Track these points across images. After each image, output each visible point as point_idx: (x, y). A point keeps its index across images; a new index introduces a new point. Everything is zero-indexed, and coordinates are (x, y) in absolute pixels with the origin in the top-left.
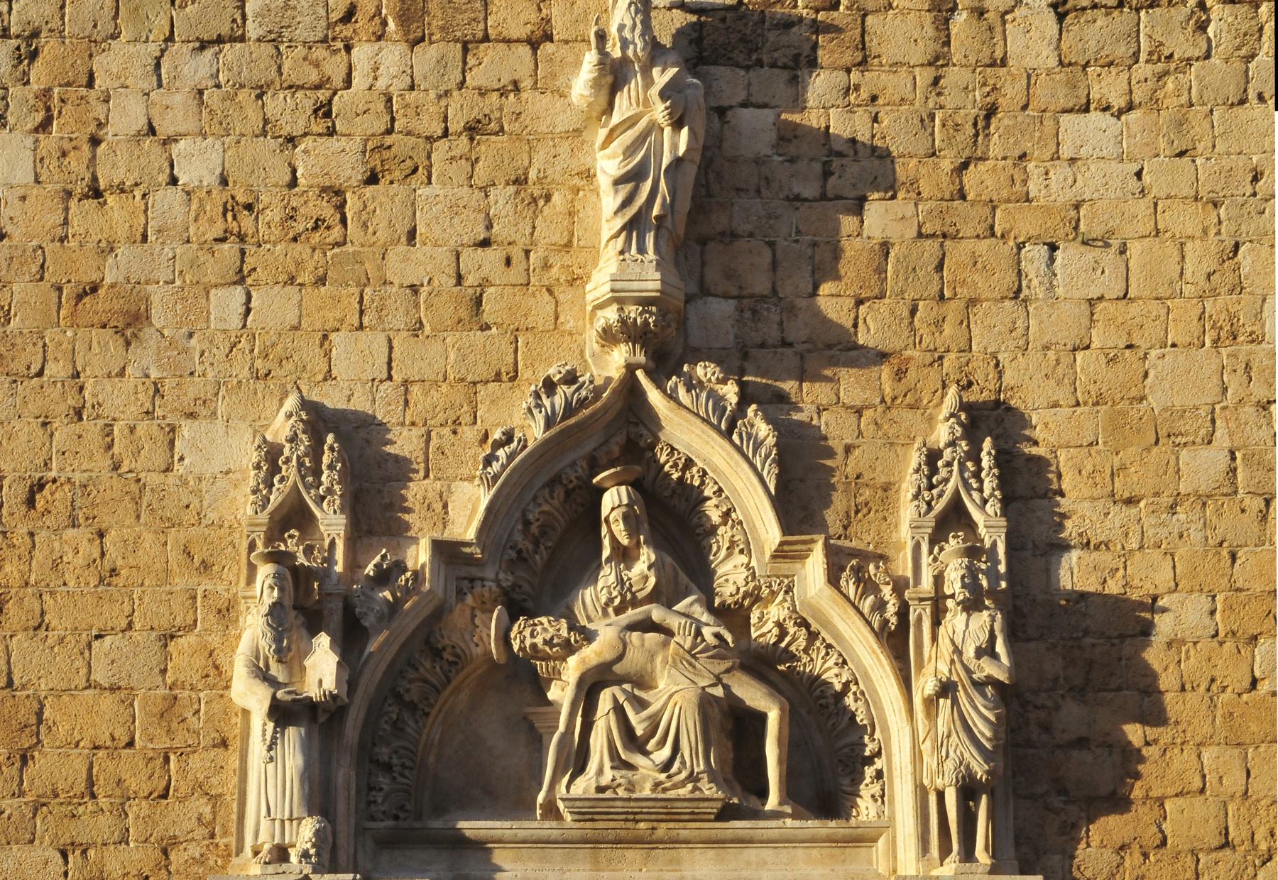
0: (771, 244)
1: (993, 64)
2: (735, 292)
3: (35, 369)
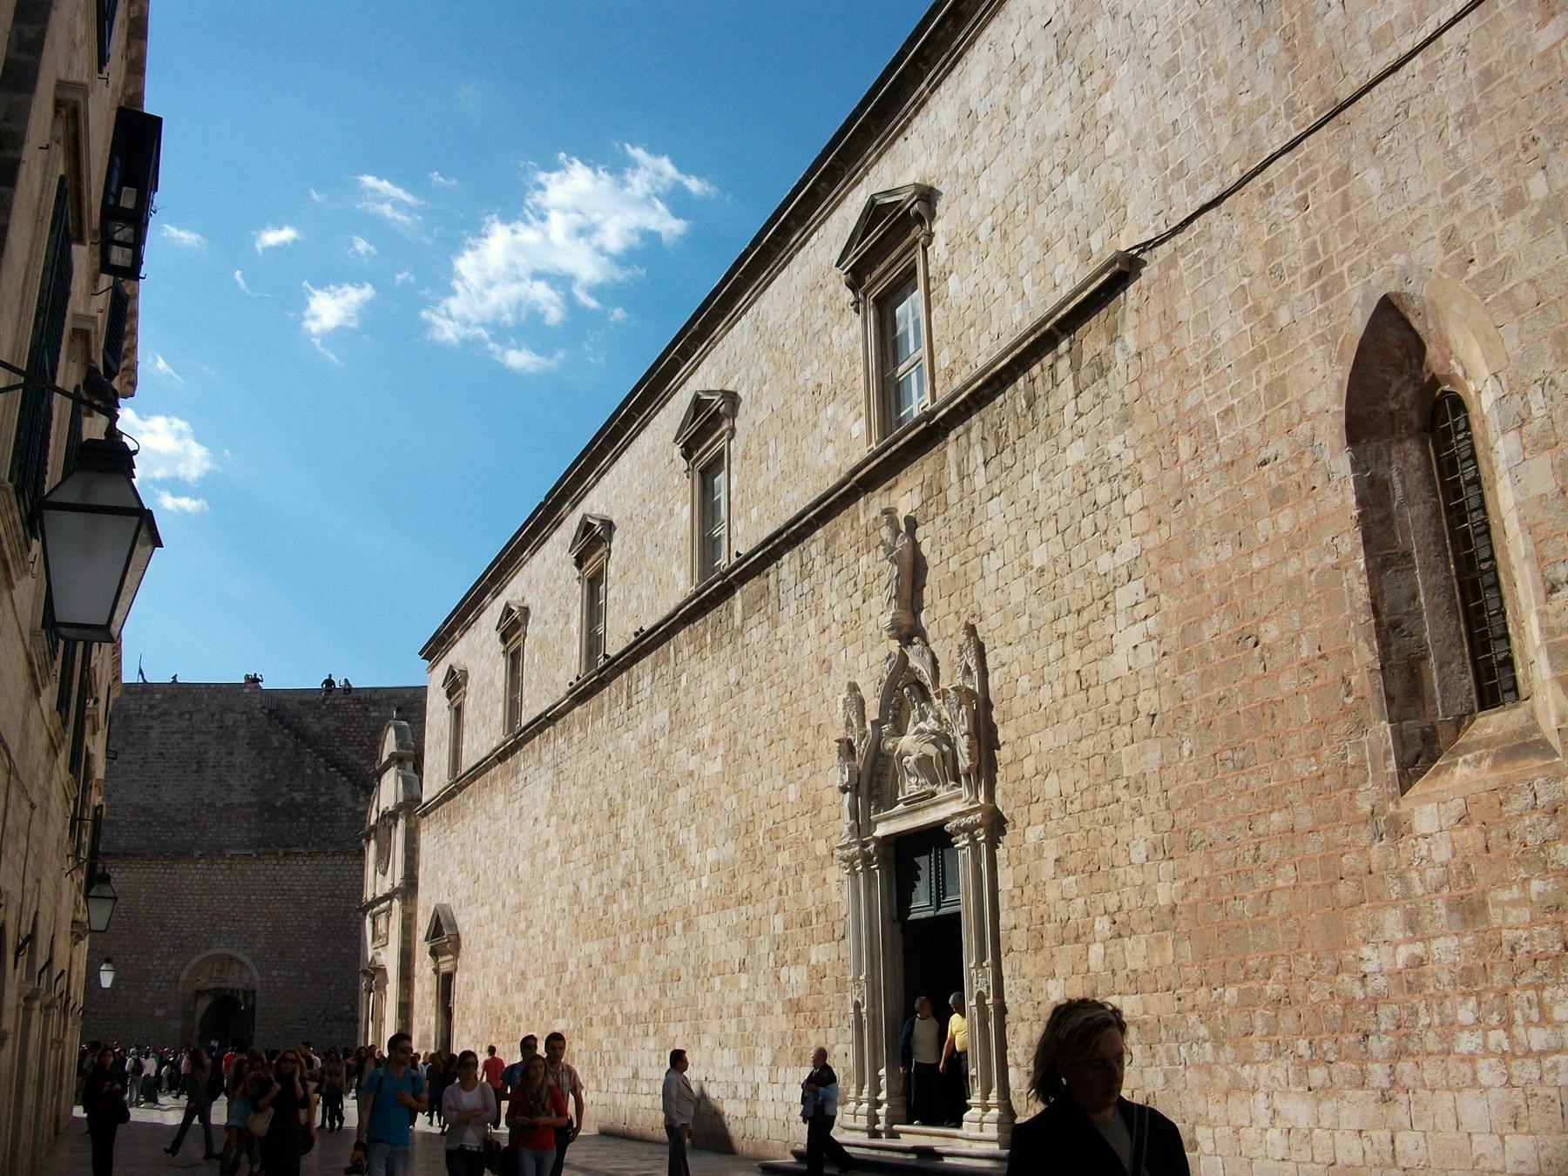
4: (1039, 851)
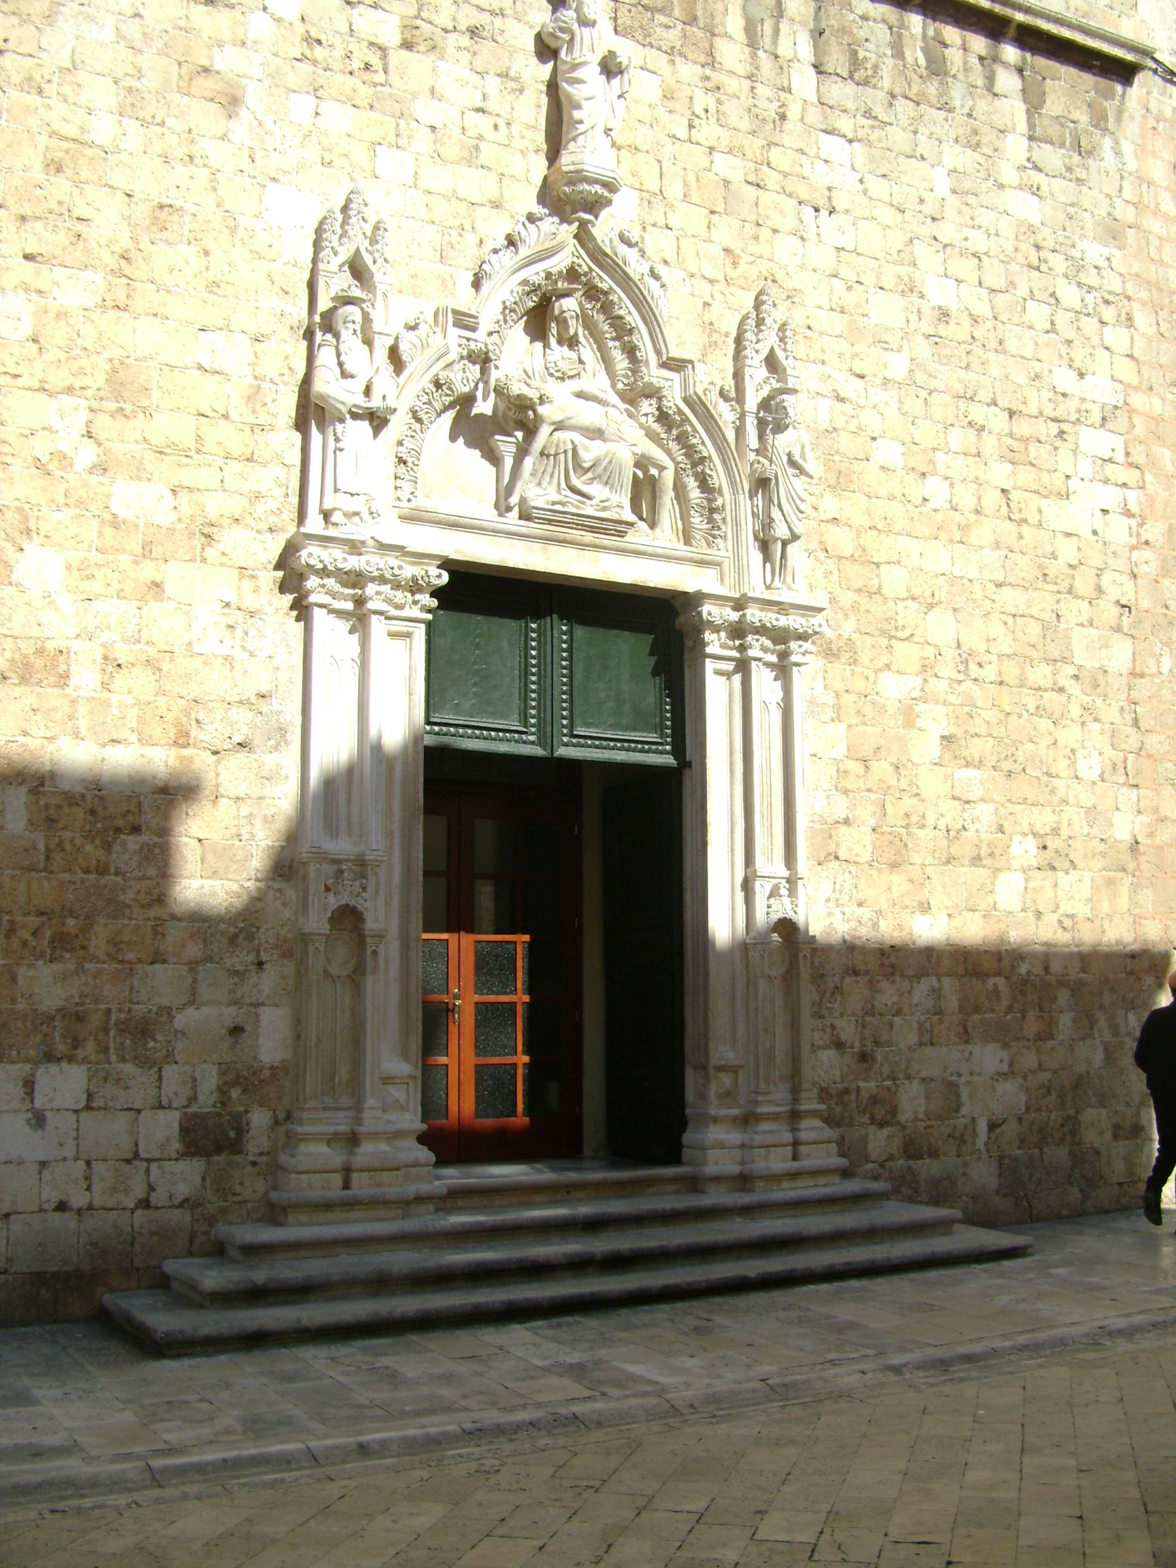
0: (659, 161)
1: (783, 90)
2: (638, 186)
3: (158, 120)
4: (909, 717)
